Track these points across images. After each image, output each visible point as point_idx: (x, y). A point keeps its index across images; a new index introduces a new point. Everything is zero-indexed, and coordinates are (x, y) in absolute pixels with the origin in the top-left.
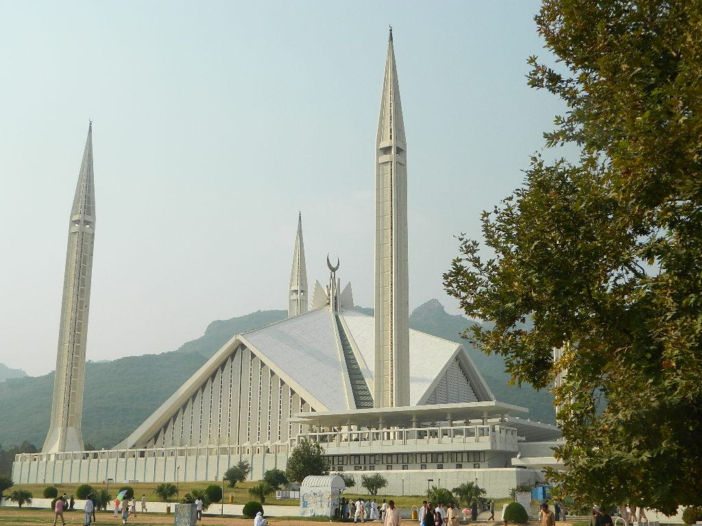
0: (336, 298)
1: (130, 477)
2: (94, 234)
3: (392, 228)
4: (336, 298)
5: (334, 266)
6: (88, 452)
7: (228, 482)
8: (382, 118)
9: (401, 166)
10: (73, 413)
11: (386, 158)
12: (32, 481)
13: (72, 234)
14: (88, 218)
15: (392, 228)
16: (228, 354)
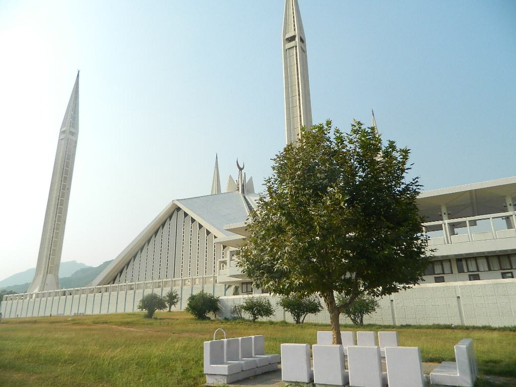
0: (243, 186)
1: (74, 311)
2: (76, 142)
3: (299, 95)
4: (243, 186)
5: (242, 167)
6: (66, 290)
7: (145, 311)
8: (286, 19)
9: (303, 51)
10: (53, 264)
11: (292, 44)
12: (13, 316)
13: (60, 140)
14: (72, 130)
15: (299, 95)
16: (167, 217)
